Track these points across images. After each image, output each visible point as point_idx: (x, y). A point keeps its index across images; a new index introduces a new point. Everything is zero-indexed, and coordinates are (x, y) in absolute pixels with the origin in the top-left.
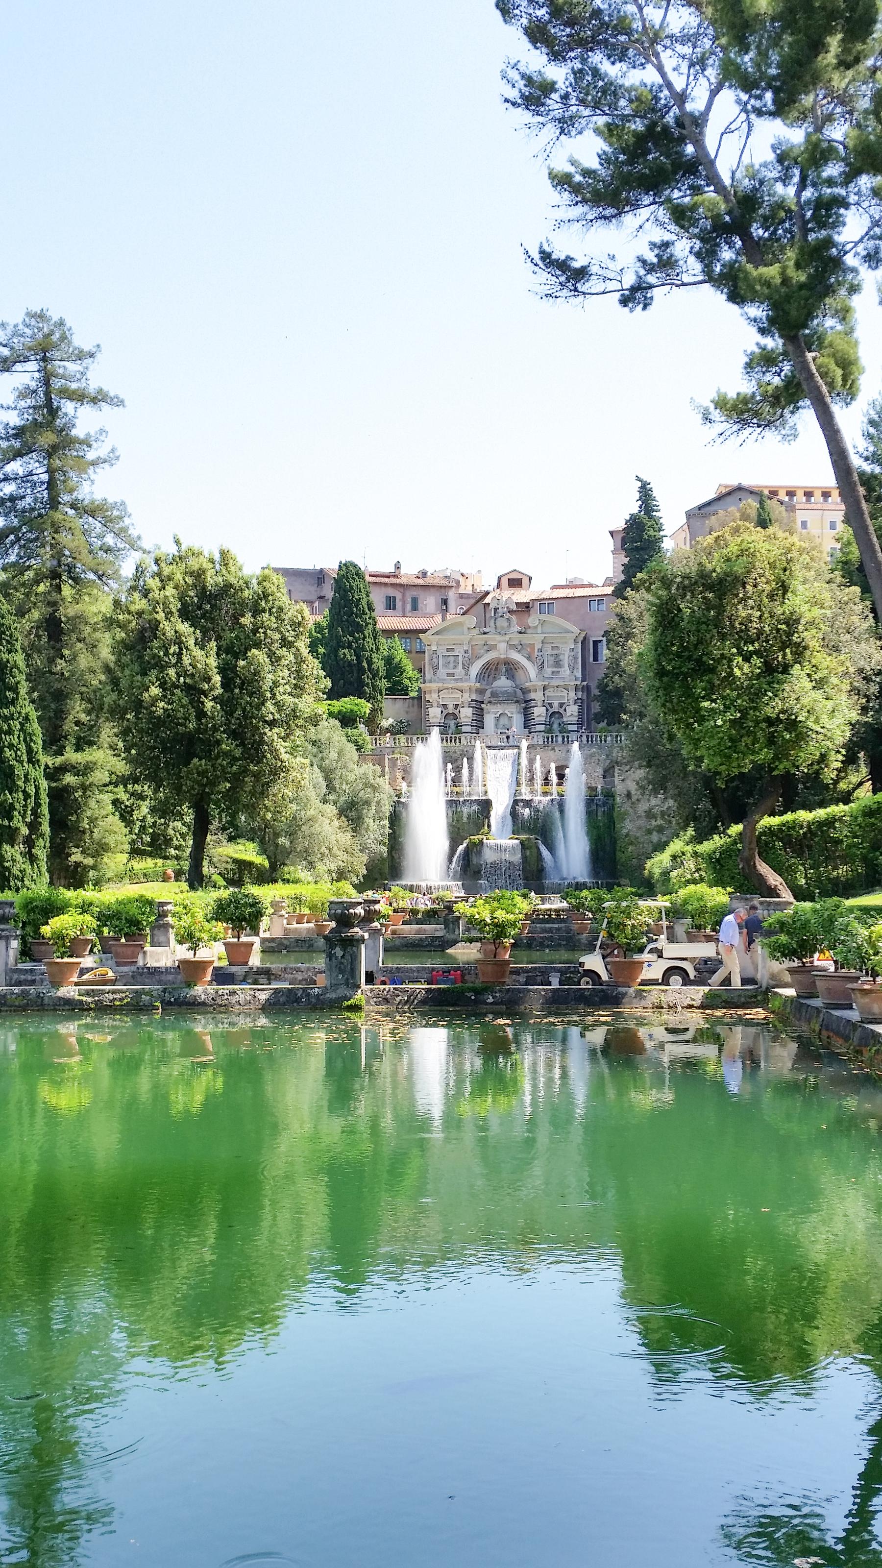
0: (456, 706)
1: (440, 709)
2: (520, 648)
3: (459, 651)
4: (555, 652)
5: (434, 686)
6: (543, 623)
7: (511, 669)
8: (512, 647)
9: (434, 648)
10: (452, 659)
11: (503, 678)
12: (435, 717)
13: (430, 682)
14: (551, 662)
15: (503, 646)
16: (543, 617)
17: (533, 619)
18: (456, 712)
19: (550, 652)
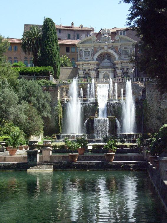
0: (89, 70)
1: (83, 71)
2: (112, 48)
3: (90, 50)
4: (125, 49)
5: (81, 63)
6: (121, 39)
7: (109, 56)
8: (109, 48)
9: (81, 48)
10: (87, 52)
11: (106, 59)
12: (81, 74)
13: (79, 61)
14: (124, 53)
15: (106, 48)
16: (121, 36)
17: (117, 37)
18: (89, 72)
19: (123, 49)
